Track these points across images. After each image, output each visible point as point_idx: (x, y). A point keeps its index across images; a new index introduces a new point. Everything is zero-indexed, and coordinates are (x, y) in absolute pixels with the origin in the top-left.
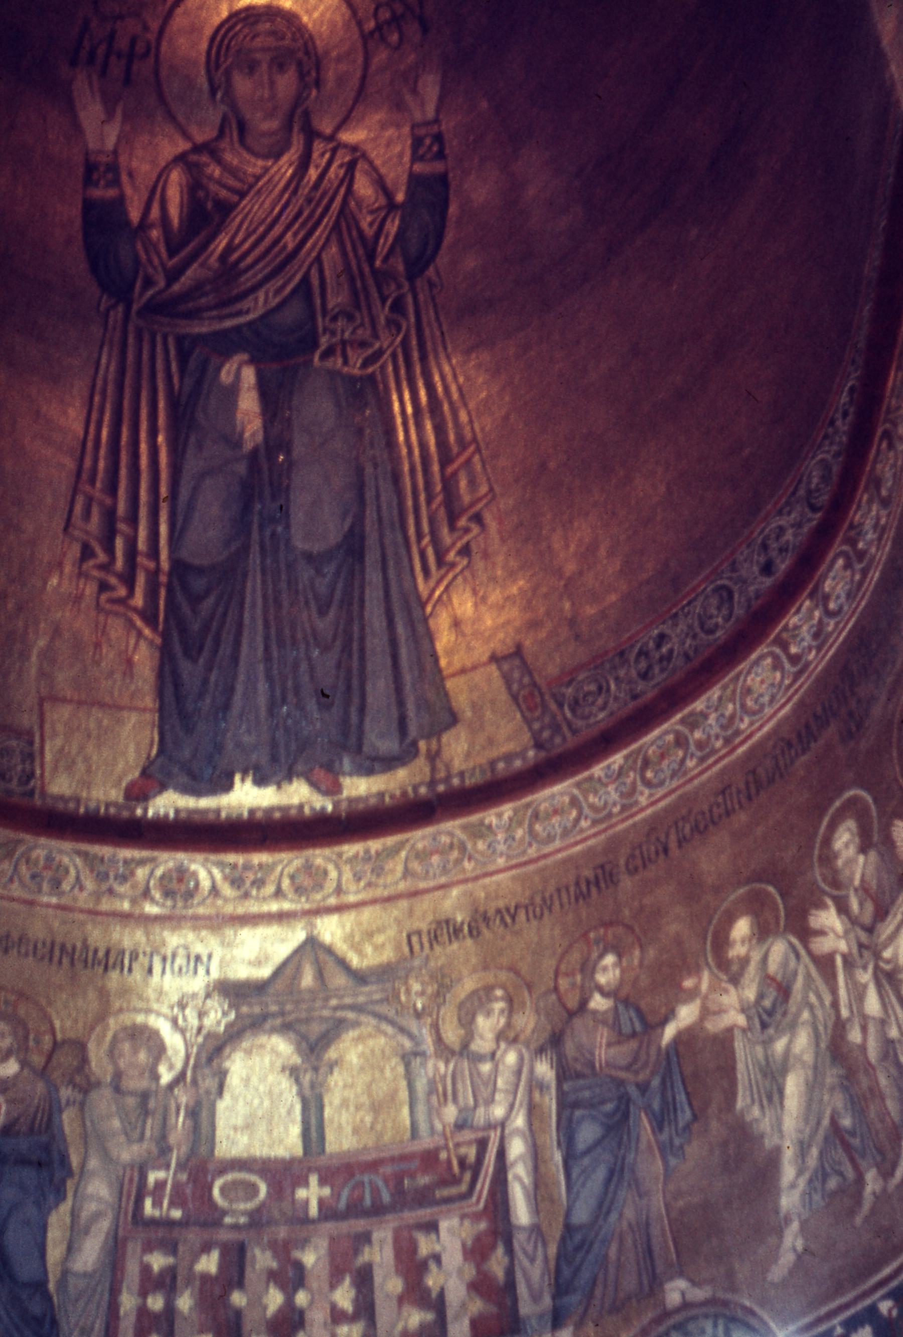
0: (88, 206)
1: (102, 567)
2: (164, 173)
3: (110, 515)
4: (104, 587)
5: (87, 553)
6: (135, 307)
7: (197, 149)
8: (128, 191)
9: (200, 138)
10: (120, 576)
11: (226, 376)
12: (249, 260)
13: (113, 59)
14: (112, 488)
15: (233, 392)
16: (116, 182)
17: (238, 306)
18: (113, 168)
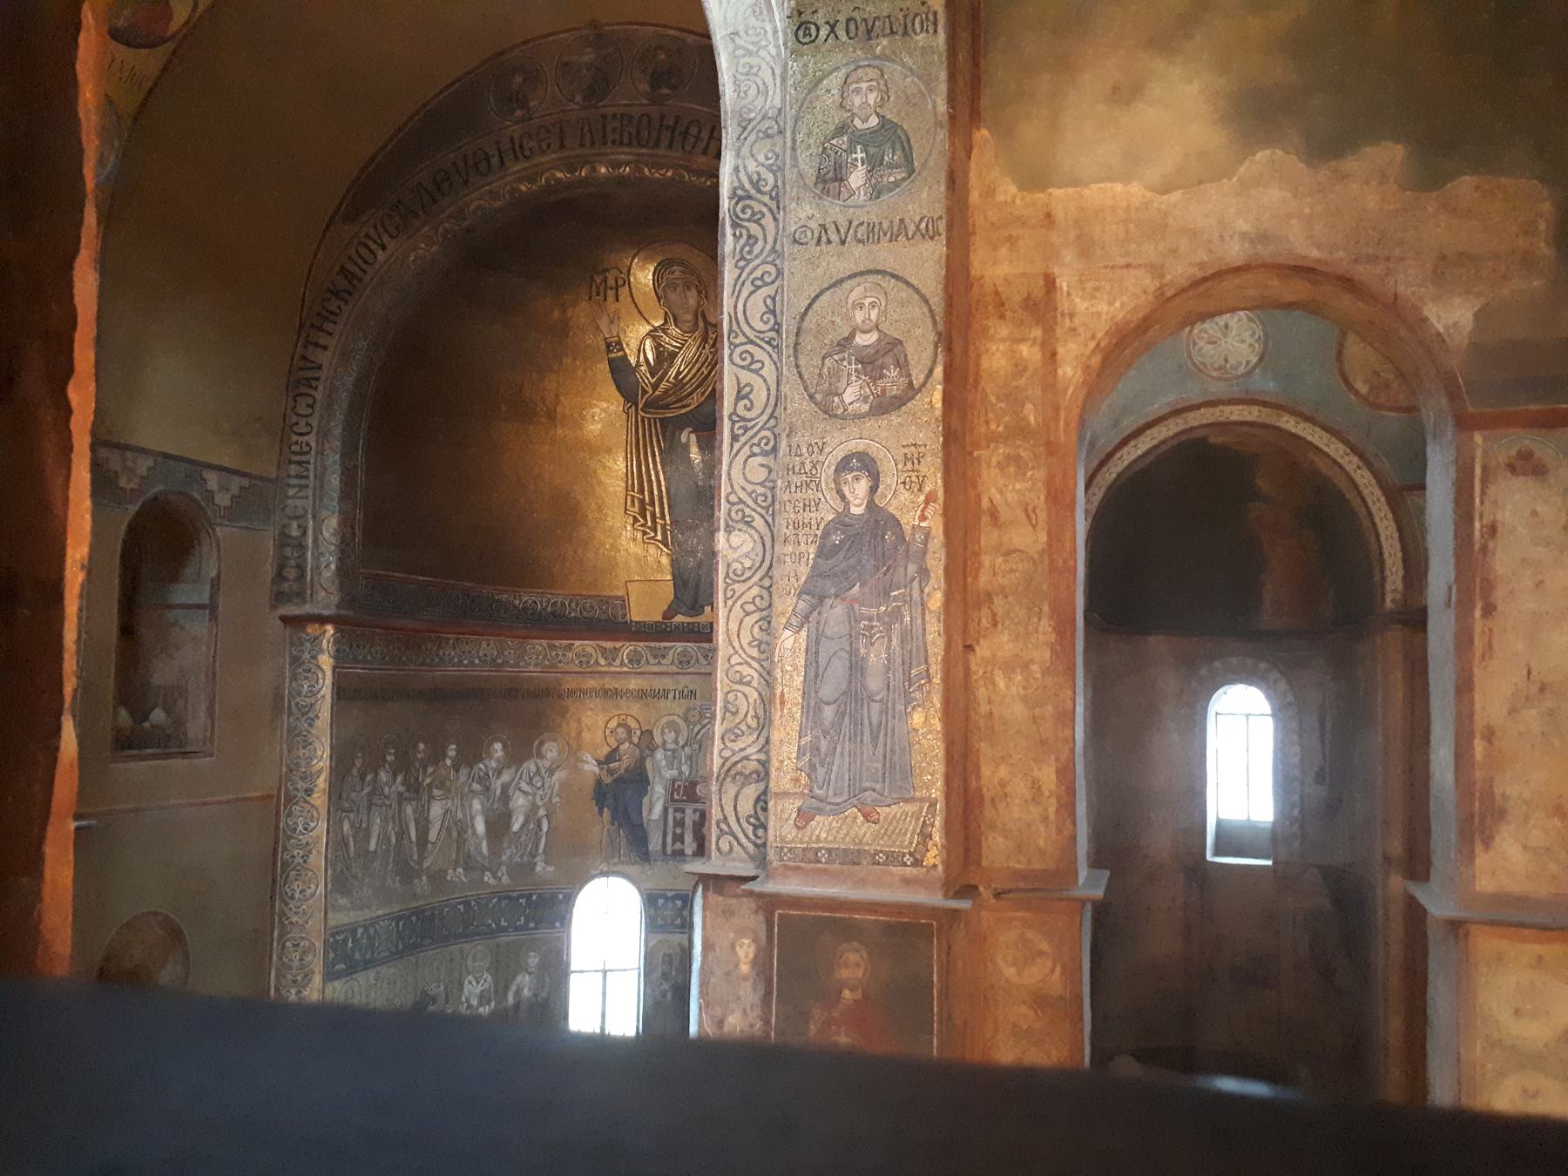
0: (611, 361)
1: (642, 525)
2: (642, 342)
3: (642, 502)
4: (645, 533)
5: (636, 521)
6: (640, 406)
7: (655, 329)
8: (627, 351)
9: (657, 325)
10: (649, 528)
11: (684, 439)
12: (687, 379)
13: (609, 291)
14: (641, 491)
15: (686, 447)
16: (622, 349)
17: (685, 402)
18: (619, 343)
